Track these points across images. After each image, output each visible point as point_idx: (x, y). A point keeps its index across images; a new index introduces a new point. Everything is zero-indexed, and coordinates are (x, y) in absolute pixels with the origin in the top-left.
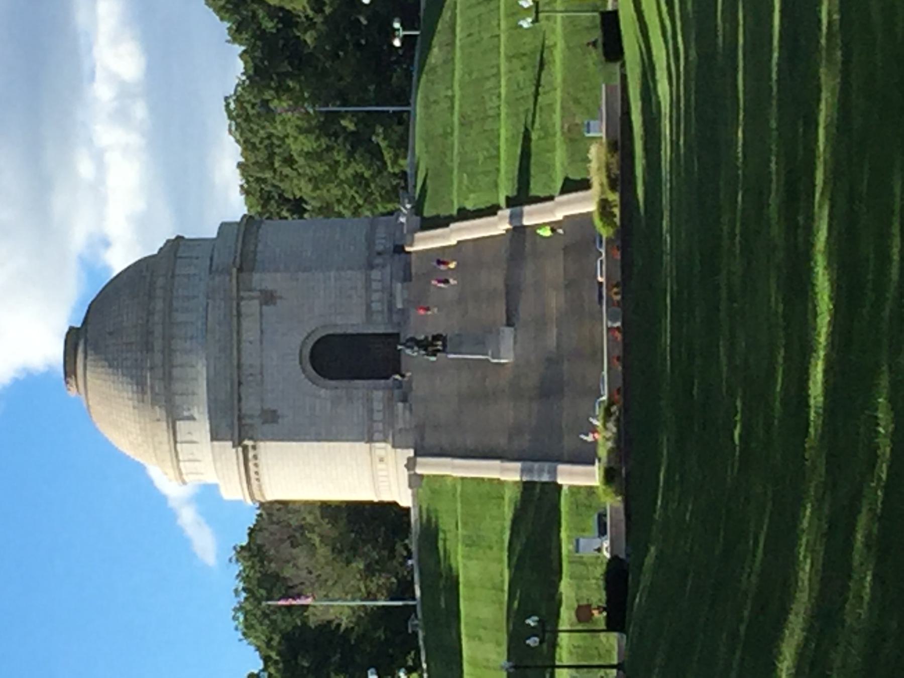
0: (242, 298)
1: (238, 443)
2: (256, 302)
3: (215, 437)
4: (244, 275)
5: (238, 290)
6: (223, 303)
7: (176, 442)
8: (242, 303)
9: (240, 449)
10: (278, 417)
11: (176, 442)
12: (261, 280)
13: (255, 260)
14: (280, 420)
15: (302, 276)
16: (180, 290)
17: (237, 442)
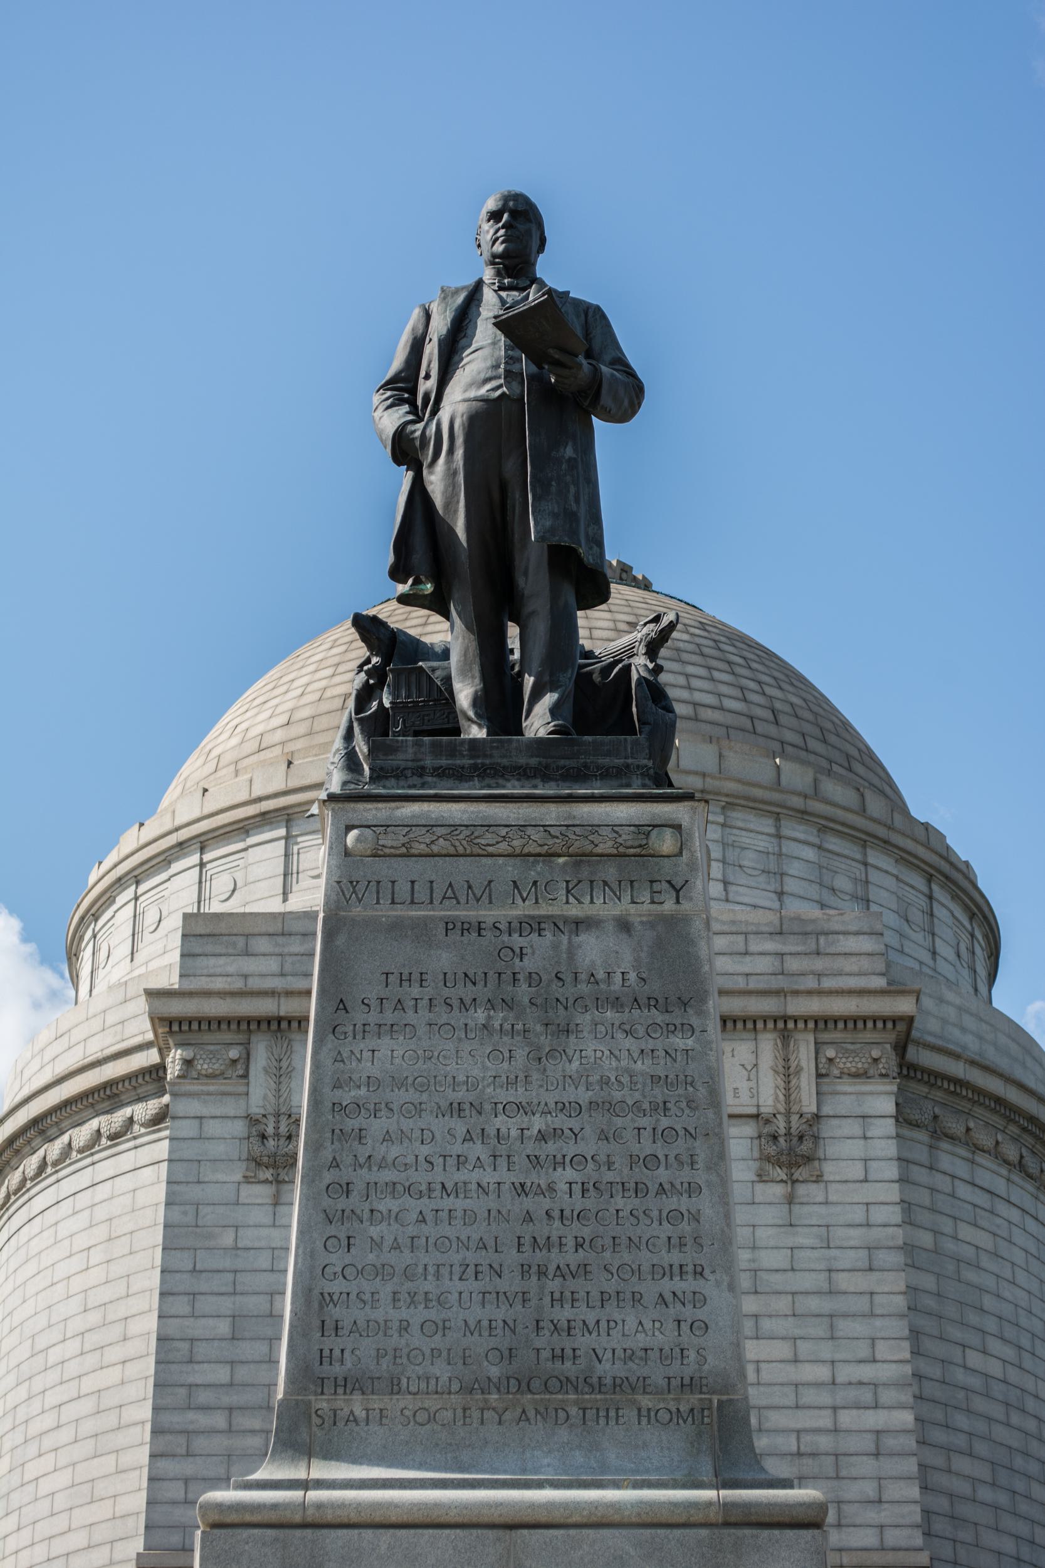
0: (785, 1037)
1: (174, 1022)
2: (768, 1097)
3: (203, 934)
4: (889, 1062)
5: (822, 1022)
6: (764, 964)
7: (203, 842)
8: (768, 1044)
9: (151, 1057)
10: (279, 1182)
11: (203, 842)
12: (864, 1129)
13: (939, 1134)
14: (261, 1193)
15: (890, 1288)
16: (810, 854)
17: (177, 1008)
